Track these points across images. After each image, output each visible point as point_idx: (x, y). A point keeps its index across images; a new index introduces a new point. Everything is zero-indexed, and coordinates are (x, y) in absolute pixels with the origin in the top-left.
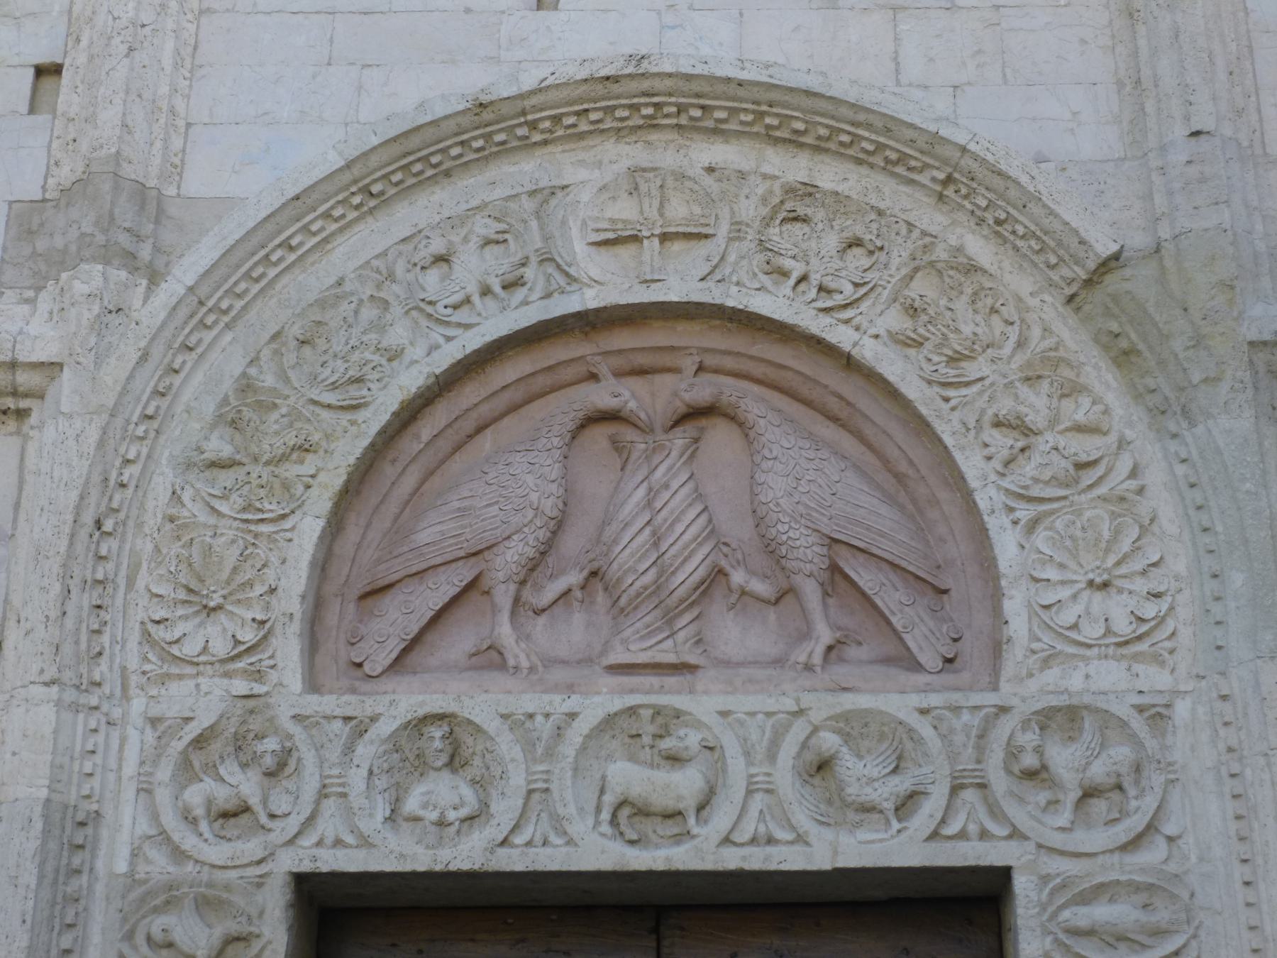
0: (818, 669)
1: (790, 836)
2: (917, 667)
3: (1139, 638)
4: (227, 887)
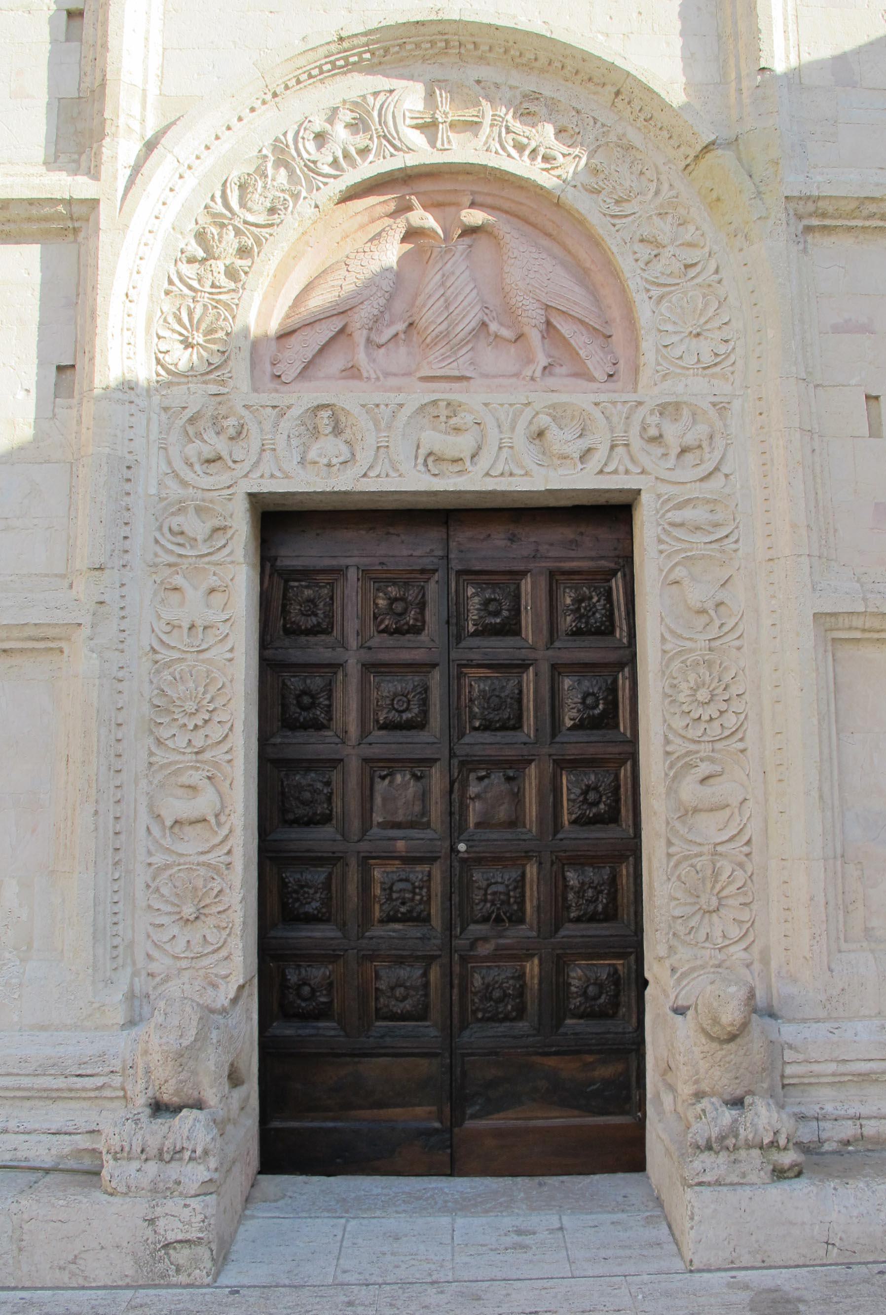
0: (538, 379)
1: (522, 472)
2: (592, 379)
3: (715, 365)
4: (211, 501)
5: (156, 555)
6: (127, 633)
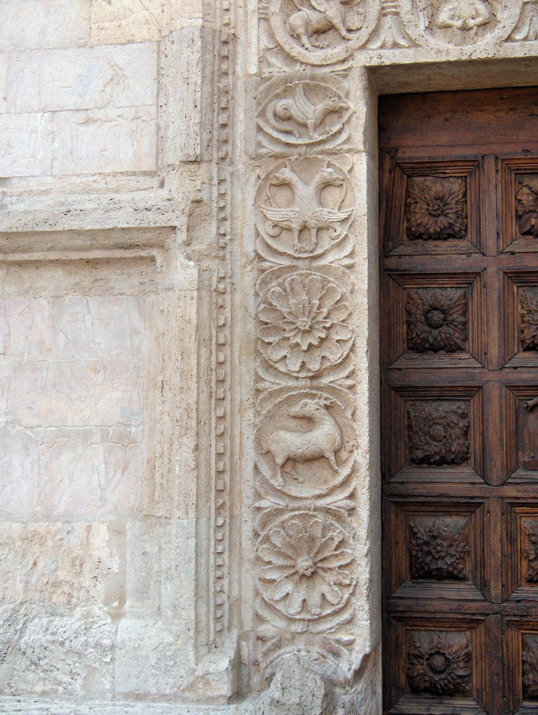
4: (323, 79)
5: (259, 145)
6: (228, 237)
